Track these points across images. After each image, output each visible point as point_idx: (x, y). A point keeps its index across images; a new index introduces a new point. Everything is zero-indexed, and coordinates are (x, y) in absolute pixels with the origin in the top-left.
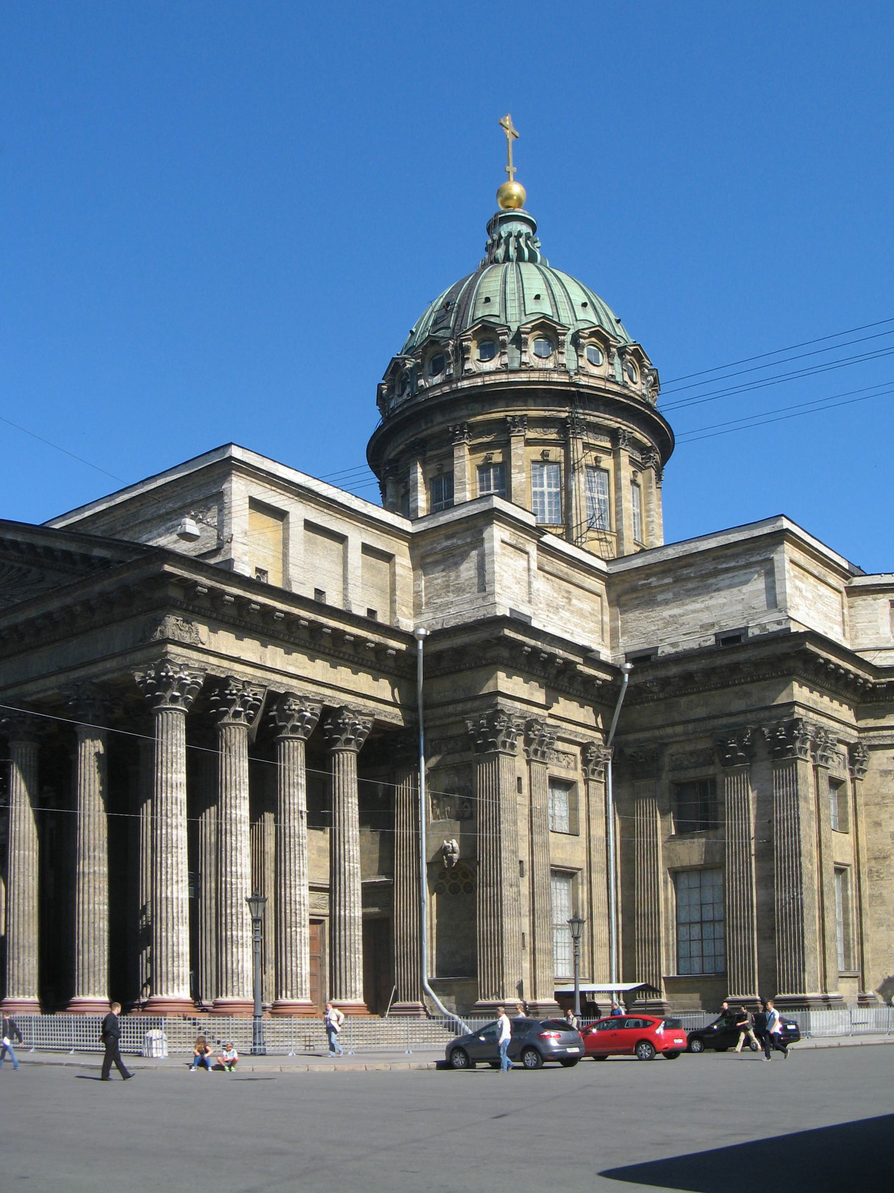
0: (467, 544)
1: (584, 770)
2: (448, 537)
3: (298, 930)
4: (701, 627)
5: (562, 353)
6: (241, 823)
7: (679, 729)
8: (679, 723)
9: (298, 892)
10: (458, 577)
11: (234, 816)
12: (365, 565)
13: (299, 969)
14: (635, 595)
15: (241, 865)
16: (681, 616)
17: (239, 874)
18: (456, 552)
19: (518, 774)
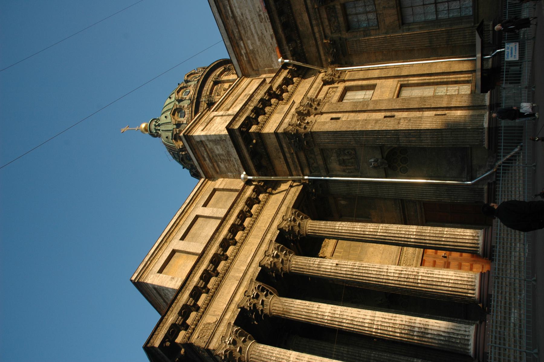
0: (206, 149)
1: (338, 83)
2: (205, 160)
3: (420, 278)
4: (261, 22)
5: (184, 106)
6: (334, 314)
7: (316, 29)
8: (313, 30)
9: (392, 275)
10: (222, 155)
11: (329, 318)
12: (214, 206)
13: (451, 281)
14: (252, 61)
15: (364, 319)
16: (258, 35)
17: (370, 322)
18: (210, 155)
19: (328, 119)
